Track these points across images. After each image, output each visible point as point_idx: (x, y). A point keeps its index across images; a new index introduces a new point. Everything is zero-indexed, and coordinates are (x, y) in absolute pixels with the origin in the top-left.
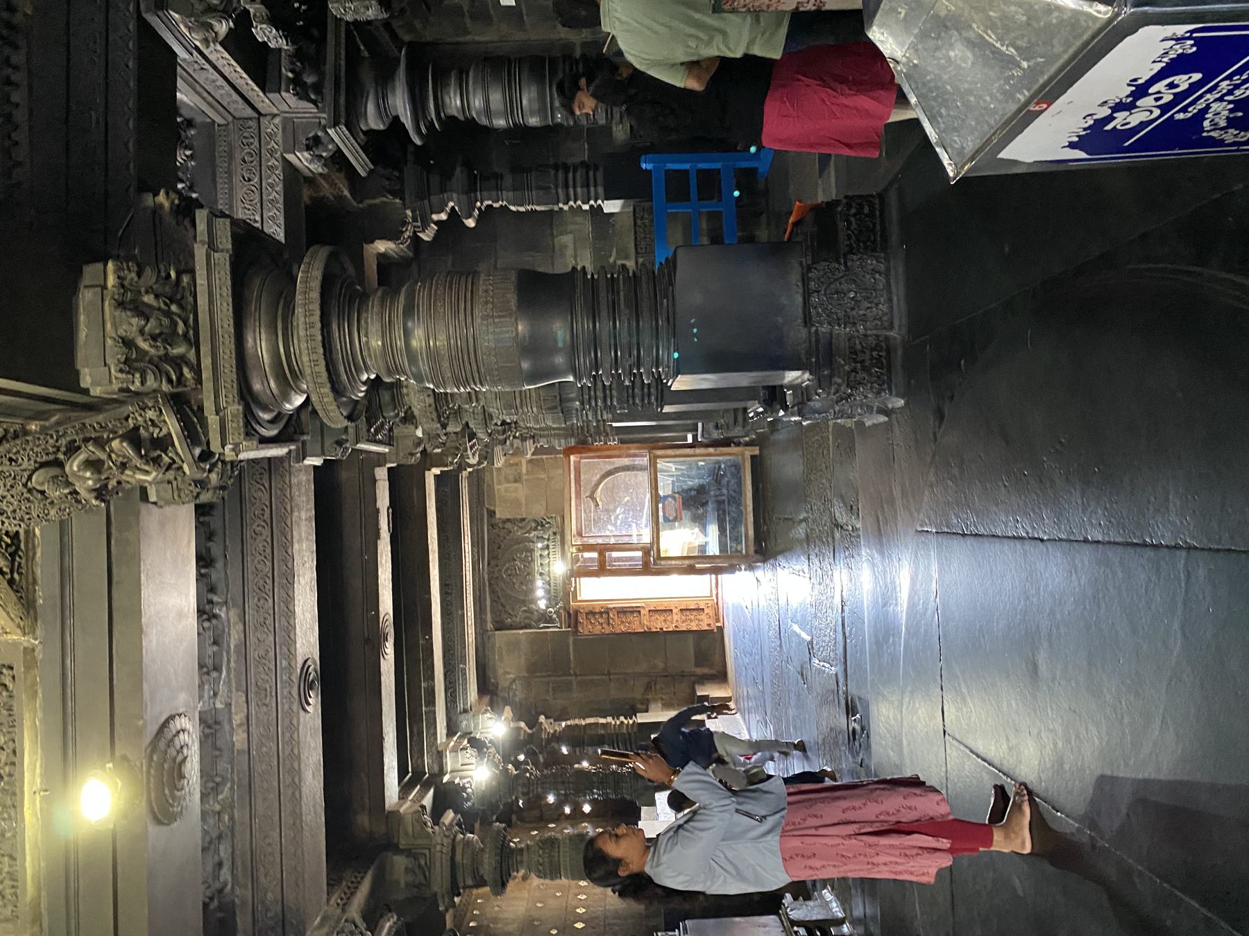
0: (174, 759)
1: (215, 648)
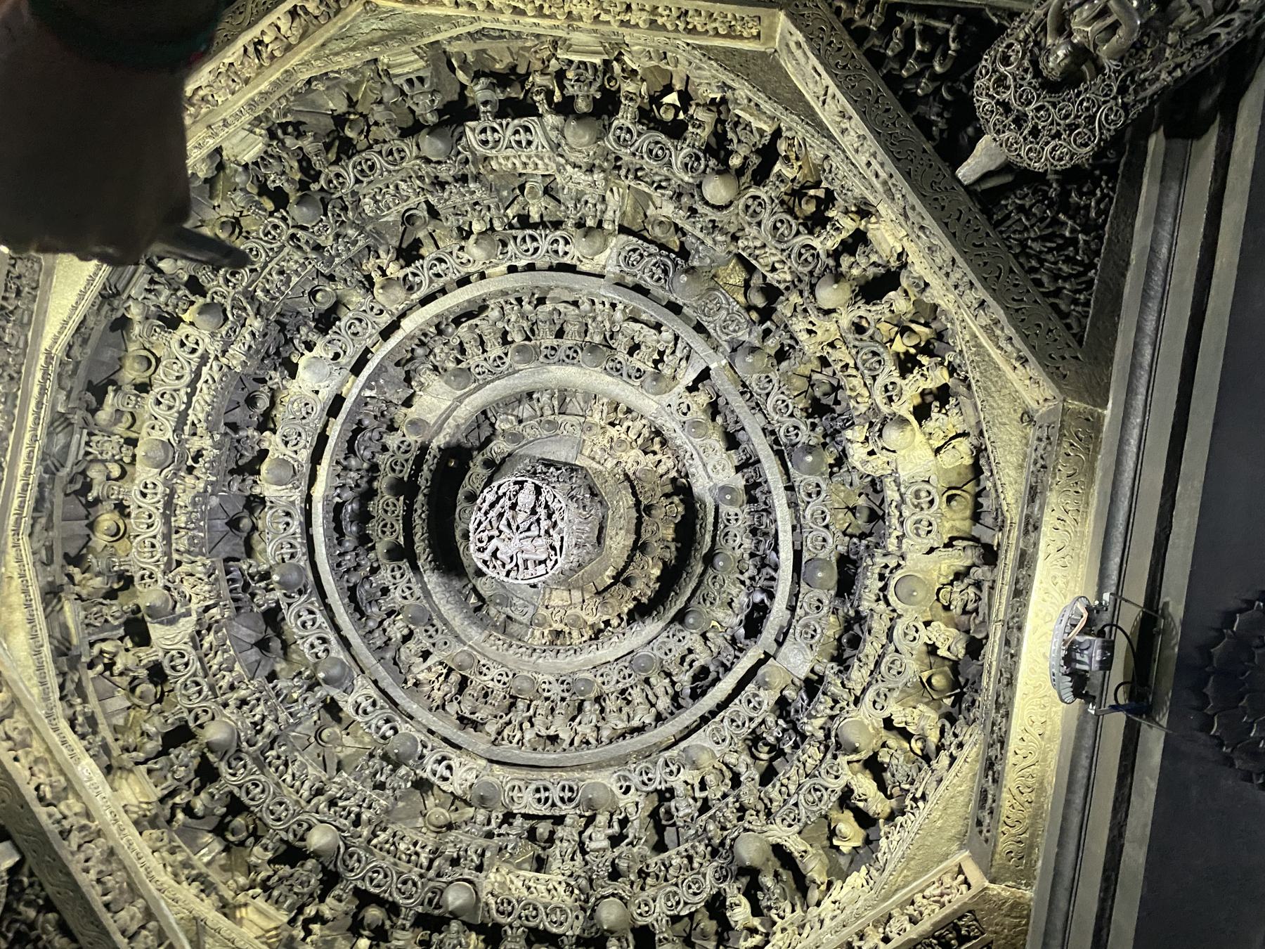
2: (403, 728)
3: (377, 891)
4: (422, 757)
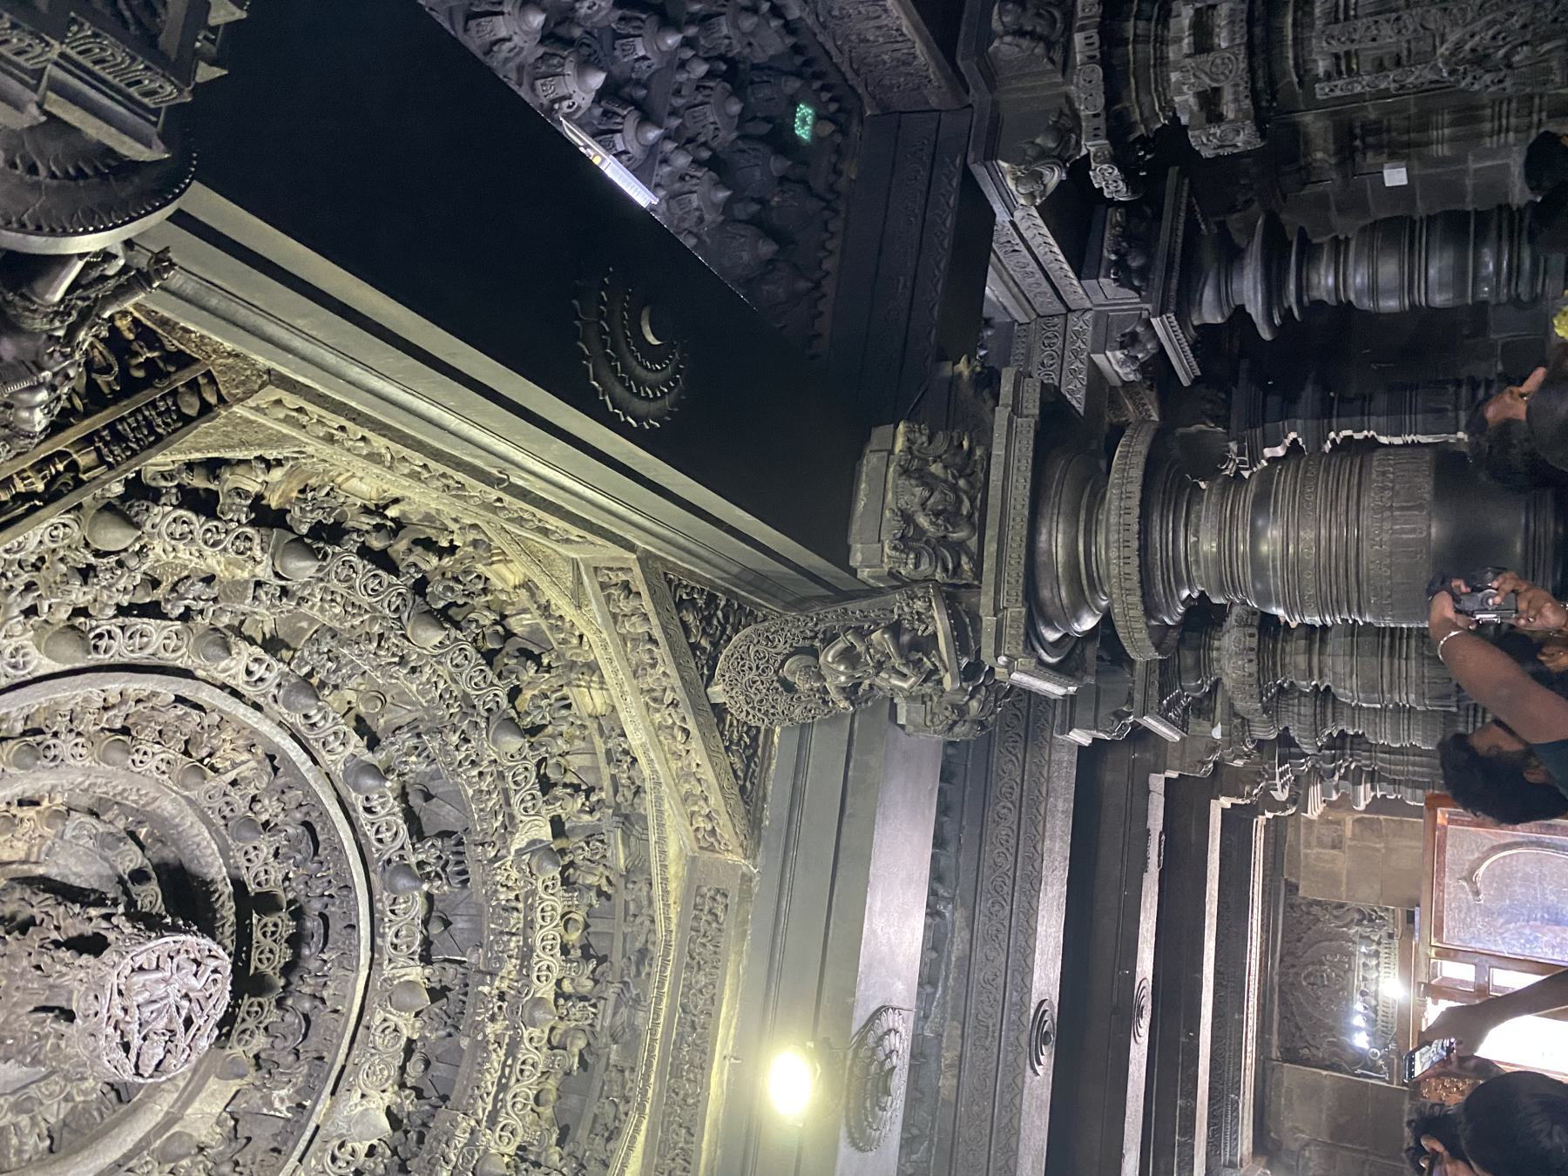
0: (882, 1064)
1: (934, 955)
2: (297, 719)
3: (379, 572)
4: (279, 685)
